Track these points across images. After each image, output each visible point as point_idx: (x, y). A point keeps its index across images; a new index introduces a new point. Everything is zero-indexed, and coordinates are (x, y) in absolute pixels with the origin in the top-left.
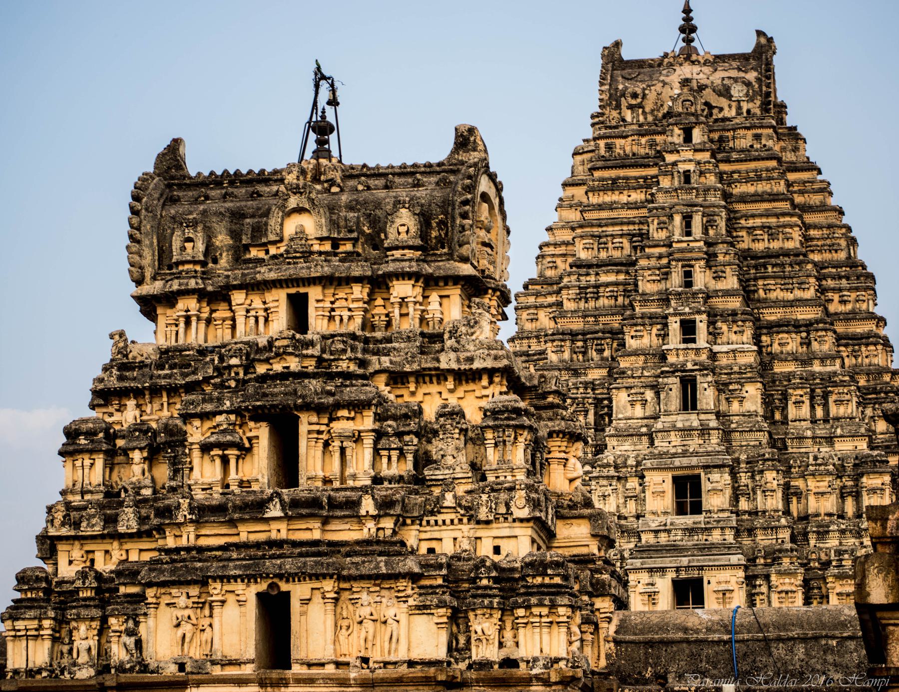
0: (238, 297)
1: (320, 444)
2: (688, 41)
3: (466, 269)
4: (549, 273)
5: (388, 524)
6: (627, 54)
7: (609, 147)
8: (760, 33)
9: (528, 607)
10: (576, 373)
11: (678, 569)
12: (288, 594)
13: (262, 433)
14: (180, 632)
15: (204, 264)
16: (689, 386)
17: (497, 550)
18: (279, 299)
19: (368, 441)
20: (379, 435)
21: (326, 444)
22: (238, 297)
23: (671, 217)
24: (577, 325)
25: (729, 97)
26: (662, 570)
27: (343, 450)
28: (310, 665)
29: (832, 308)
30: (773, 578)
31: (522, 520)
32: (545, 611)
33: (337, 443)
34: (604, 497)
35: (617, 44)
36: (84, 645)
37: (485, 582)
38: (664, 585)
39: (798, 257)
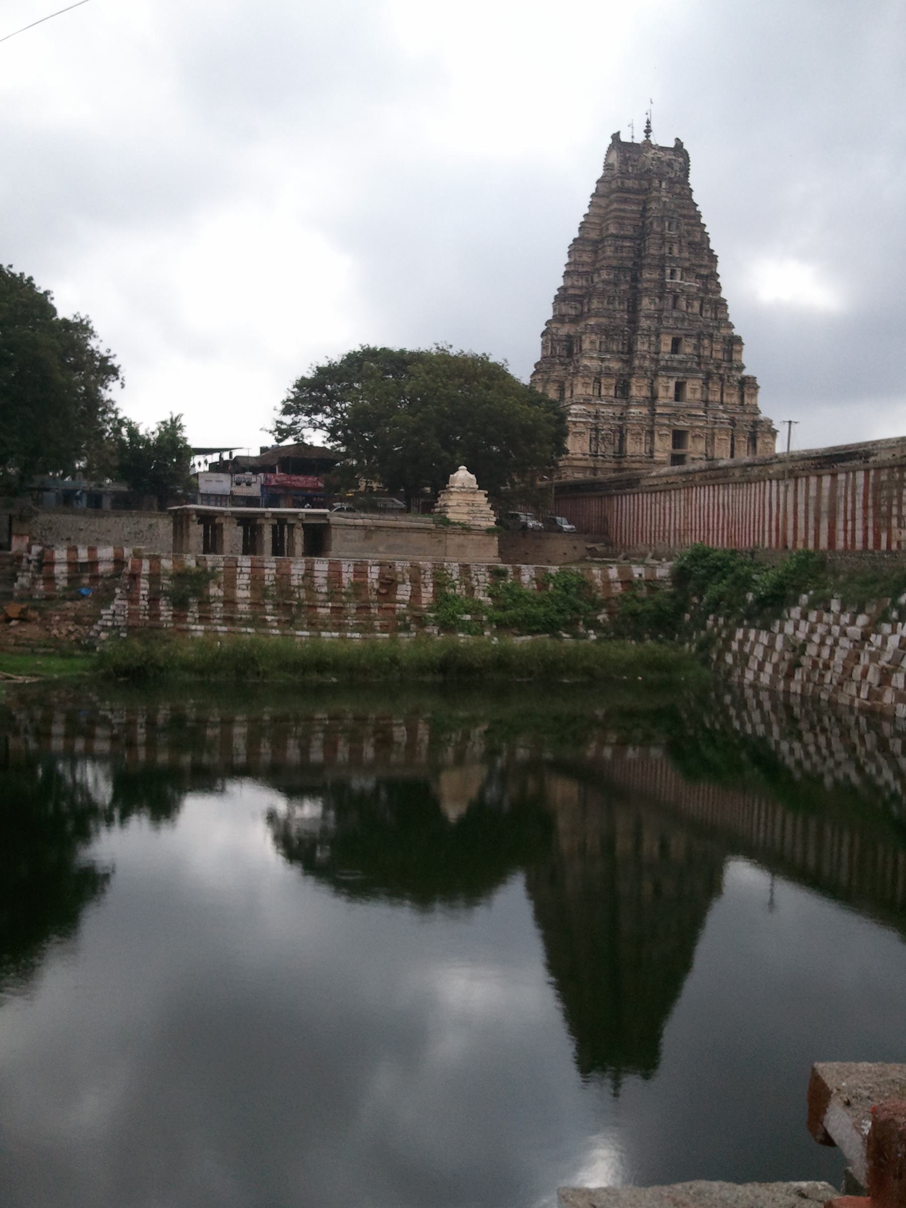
2: (647, 137)
4: (586, 236)
6: (625, 138)
7: (623, 183)
8: (677, 139)
10: (616, 285)
11: (678, 378)
16: (676, 298)
23: (663, 222)
24: (614, 263)
25: (673, 168)
26: (672, 377)
30: (710, 385)
34: (643, 343)
35: (618, 133)
38: (672, 384)
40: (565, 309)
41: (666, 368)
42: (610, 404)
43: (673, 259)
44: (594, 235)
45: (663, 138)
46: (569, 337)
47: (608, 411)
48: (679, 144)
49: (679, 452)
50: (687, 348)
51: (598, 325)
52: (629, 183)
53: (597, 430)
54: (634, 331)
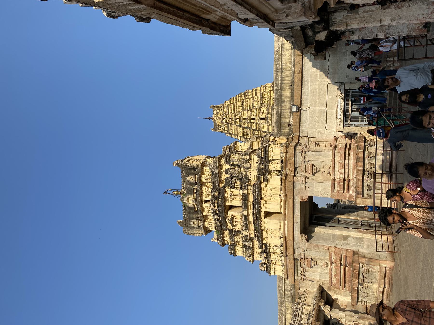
0: (205, 214)
1: (233, 200)
3: (199, 166)
5: (249, 187)
9: (268, 157)
12: (265, 212)
13: (230, 213)
14: (273, 237)
15: (199, 220)
16: (261, 119)
17: (257, 163)
18: (205, 205)
19: (232, 190)
20: (231, 187)
21: (233, 199)
22: (205, 214)
27: (234, 196)
28: (281, 208)
29: (251, 97)
31: (250, 157)
32: (269, 153)
33: (233, 197)
36: (276, 258)
37: (263, 166)
39: (243, 102)
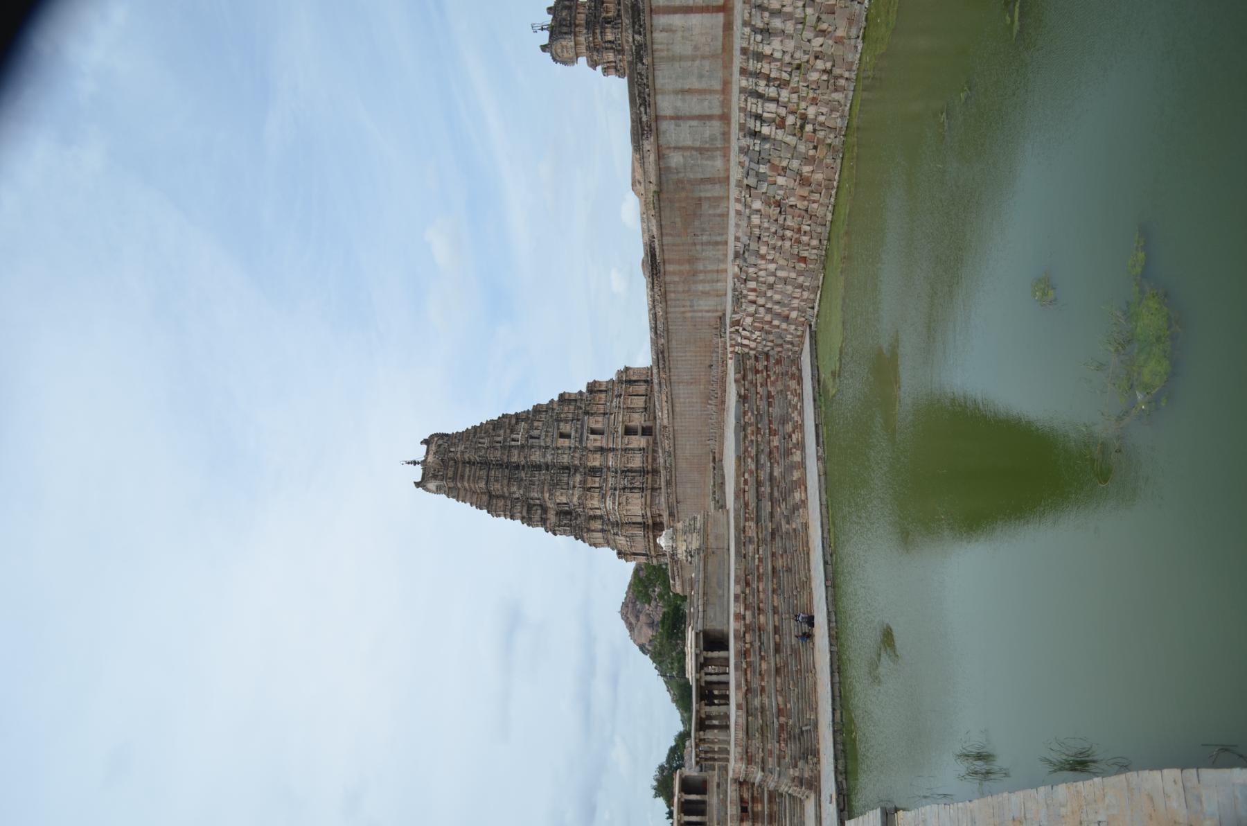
6: (419, 479)
16: (532, 437)
24: (505, 482)
38: (592, 437)
40: (537, 517)
41: (581, 441)
42: (606, 480)
43: (505, 440)
44: (485, 498)
45: (420, 452)
46: (558, 514)
47: (611, 481)
48: (426, 442)
49: (640, 431)
50: (566, 428)
51: (550, 490)
52: (450, 474)
53: (624, 489)
54: (554, 465)
